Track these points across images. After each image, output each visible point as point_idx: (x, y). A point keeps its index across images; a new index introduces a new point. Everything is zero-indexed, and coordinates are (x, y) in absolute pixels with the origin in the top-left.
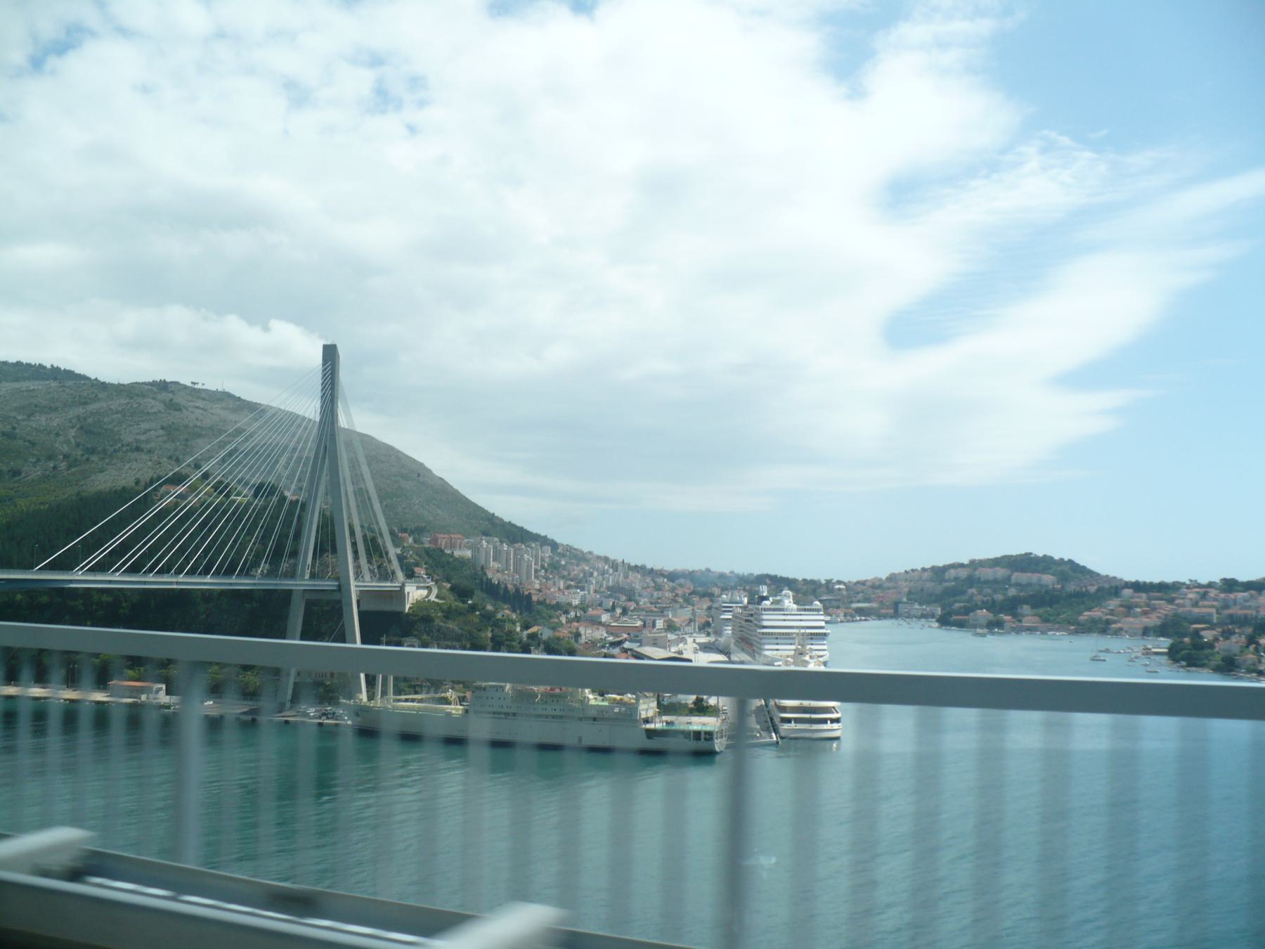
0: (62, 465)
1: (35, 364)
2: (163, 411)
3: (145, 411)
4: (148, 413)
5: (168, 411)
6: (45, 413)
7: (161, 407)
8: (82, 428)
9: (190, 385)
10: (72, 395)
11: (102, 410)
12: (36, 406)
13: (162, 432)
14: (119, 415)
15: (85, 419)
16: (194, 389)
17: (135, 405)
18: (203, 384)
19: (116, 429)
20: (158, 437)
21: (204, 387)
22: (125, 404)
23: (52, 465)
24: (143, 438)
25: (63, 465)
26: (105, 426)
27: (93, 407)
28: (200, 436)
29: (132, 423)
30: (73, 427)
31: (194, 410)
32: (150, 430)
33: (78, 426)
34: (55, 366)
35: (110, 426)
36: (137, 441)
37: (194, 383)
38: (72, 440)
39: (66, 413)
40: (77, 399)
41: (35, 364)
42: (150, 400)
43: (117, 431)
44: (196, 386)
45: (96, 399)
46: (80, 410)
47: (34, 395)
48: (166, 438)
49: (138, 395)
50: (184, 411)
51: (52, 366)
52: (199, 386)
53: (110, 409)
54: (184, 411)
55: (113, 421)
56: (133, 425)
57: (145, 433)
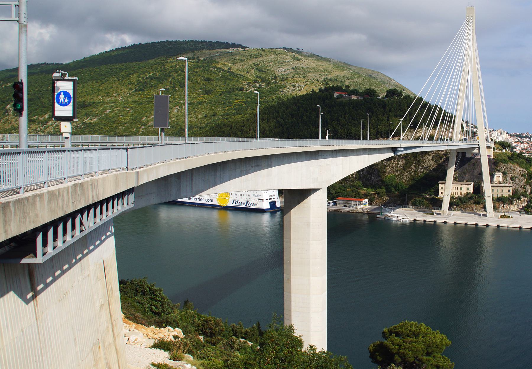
0: (263, 85)
1: (225, 42)
2: (292, 61)
3: (284, 61)
4: (285, 62)
5: (294, 61)
6: (239, 63)
7: (290, 59)
8: (257, 69)
9: (297, 50)
10: (249, 54)
11: (264, 61)
12: (235, 59)
13: (293, 71)
14: (273, 63)
15: (258, 65)
16: (299, 52)
17: (279, 59)
18: (302, 49)
19: (272, 70)
20: (292, 73)
21: (303, 51)
22: (274, 58)
23: (258, 85)
24: (285, 73)
25: (264, 85)
26: (267, 68)
27: (260, 59)
28: (310, 72)
29: (279, 67)
30: (253, 69)
31: (305, 60)
32: (287, 70)
33: (255, 68)
34: (233, 43)
35: (269, 68)
36: (283, 75)
37: (297, 49)
38: (254, 75)
39: (248, 62)
40: (252, 56)
41: (225, 42)
42: (286, 56)
43: (273, 70)
44: (299, 50)
45: (261, 56)
46: (255, 61)
47: (232, 54)
48: (295, 73)
49: (279, 53)
50: (301, 61)
51: (232, 43)
52: (301, 50)
53: (269, 60)
54: (301, 61)
55: (270, 66)
56: (280, 68)
57: (285, 71)
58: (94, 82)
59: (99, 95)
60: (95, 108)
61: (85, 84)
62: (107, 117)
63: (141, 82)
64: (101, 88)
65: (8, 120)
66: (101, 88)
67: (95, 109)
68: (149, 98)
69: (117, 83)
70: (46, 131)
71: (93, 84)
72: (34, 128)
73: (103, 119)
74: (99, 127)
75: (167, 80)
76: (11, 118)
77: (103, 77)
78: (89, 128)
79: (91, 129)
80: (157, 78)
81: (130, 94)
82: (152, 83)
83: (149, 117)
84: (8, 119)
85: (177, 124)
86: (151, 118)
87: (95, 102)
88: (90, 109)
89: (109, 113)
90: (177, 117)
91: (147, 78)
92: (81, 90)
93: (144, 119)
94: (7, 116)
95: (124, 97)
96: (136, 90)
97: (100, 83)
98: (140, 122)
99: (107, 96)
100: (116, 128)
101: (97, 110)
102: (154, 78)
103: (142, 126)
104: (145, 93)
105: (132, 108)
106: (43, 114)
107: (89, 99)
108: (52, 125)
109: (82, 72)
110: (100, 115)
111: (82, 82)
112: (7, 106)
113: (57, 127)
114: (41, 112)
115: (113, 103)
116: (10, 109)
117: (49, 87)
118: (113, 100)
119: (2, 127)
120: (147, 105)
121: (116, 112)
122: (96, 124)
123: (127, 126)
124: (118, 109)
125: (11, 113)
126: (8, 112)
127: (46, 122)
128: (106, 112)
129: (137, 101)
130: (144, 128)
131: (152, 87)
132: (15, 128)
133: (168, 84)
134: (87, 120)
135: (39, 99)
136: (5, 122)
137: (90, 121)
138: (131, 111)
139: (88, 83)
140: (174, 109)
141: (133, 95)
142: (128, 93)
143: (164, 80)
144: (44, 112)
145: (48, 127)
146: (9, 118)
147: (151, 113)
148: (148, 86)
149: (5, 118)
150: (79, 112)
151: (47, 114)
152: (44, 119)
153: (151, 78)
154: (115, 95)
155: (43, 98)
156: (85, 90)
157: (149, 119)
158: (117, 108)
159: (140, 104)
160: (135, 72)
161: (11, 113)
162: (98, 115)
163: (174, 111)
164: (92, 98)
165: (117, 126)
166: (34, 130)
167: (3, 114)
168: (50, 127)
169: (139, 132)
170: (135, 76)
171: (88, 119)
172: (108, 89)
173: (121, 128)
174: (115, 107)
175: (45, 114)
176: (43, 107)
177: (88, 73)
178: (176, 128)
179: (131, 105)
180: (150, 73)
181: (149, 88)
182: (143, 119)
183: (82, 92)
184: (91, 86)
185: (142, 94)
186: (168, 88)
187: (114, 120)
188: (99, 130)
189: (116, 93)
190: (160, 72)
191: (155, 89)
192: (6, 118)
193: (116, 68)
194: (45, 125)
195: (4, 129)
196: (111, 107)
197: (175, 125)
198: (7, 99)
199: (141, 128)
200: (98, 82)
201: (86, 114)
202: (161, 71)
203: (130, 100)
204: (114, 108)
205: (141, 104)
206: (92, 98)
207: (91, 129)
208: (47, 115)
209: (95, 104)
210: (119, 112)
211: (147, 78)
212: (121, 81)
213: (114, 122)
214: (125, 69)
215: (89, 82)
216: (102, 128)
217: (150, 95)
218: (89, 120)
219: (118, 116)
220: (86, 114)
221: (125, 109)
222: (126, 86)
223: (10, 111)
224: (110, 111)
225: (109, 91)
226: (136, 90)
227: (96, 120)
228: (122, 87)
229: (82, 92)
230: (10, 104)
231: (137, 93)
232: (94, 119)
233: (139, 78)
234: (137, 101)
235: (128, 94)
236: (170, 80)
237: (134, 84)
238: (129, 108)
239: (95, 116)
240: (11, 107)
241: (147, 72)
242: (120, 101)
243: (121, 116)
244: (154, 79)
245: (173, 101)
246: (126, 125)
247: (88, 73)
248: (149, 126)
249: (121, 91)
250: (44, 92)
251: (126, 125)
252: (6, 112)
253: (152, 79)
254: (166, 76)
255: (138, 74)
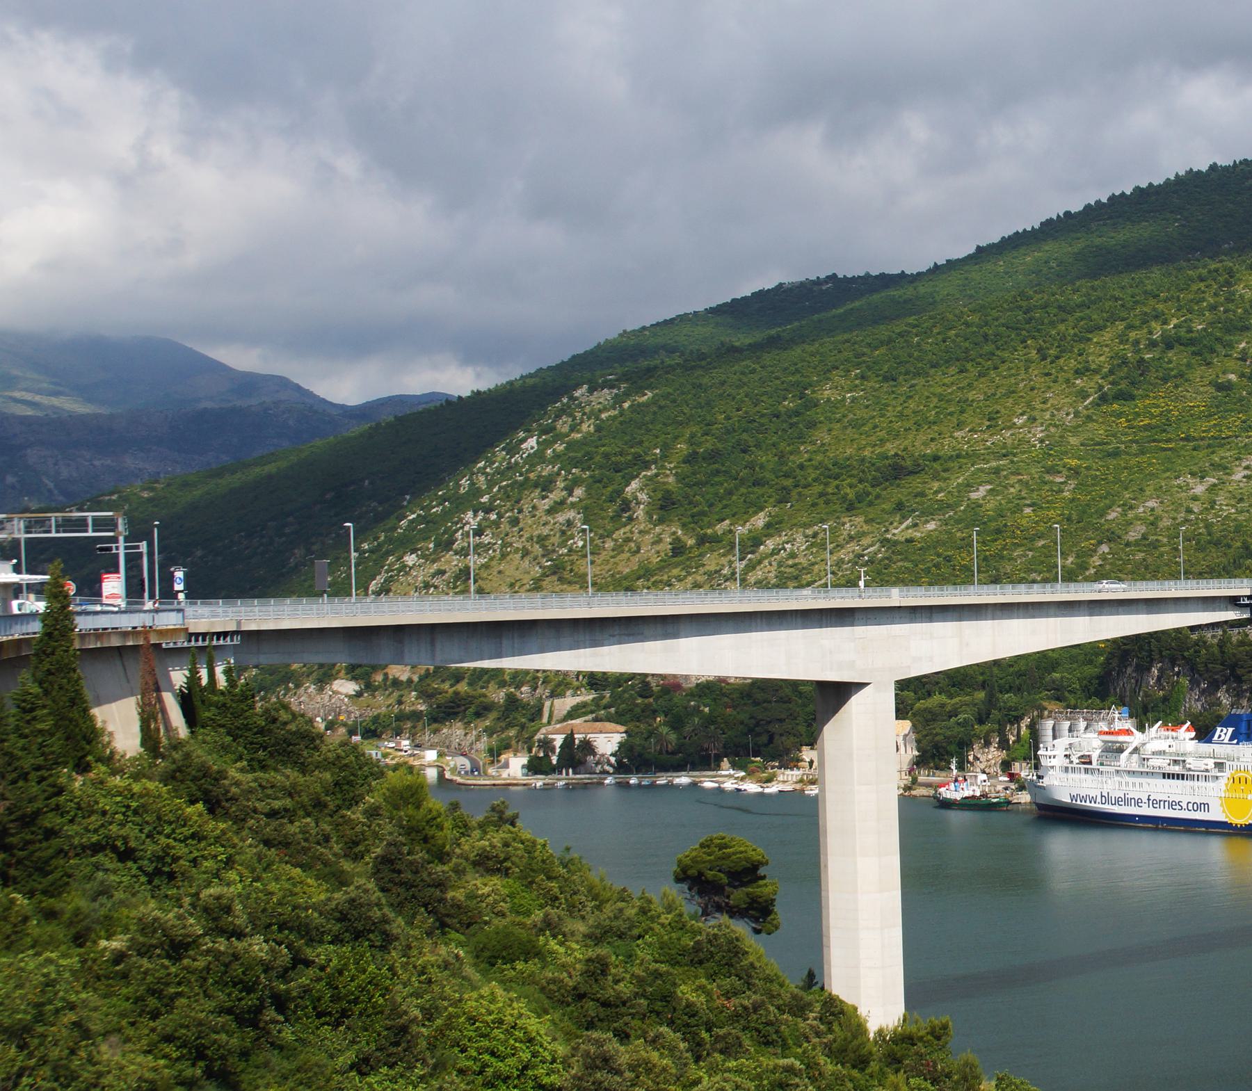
58: (953, 370)
59: (959, 426)
60: (936, 477)
61: (919, 381)
62: (974, 515)
63: (1125, 362)
64: (971, 395)
65: (628, 540)
66: (971, 395)
67: (936, 485)
68: (1148, 428)
69: (1034, 371)
70: (752, 578)
71: (945, 381)
72: (713, 568)
73: (958, 522)
74: (939, 555)
75: (1230, 345)
76: (640, 532)
77: (989, 348)
78: (902, 560)
79: (907, 564)
80: (1192, 342)
81: (1077, 414)
82: (1170, 362)
83: (1131, 508)
84: (629, 535)
85: (1238, 530)
86: (1141, 510)
87: (941, 454)
88: (916, 483)
89: (984, 498)
90: (1241, 500)
91: (1153, 344)
92: (900, 408)
93: (1112, 515)
94: (625, 526)
95: (1053, 430)
96: (1104, 399)
97: (973, 371)
98: (1097, 529)
99: (988, 427)
100: (1002, 557)
101: (943, 485)
102: (1179, 341)
103: (1100, 543)
104: (1136, 406)
105: (1075, 472)
106: (751, 510)
107: (919, 444)
108: (775, 552)
109: (914, 331)
110: (949, 506)
111: (907, 373)
112: (628, 484)
113: (790, 562)
114: (745, 501)
115: (1004, 456)
116: (636, 498)
117: (785, 399)
118: (1009, 441)
119: (607, 568)
120: (1136, 455)
121: (1012, 490)
122: (932, 543)
123: (1043, 546)
124: (1021, 480)
125: (640, 513)
126: (629, 509)
127: (755, 541)
128: (974, 496)
129: (1099, 444)
130: (1107, 550)
131: (1165, 380)
132: (647, 570)
133: (1231, 364)
134: (900, 531)
135: (744, 451)
136: (618, 549)
137: (911, 533)
138: (1072, 484)
139: (927, 375)
140: (1236, 469)
141: (1089, 418)
142: (1071, 410)
143: (1219, 347)
144: (752, 504)
145: (760, 562)
146: (632, 532)
147: (1142, 490)
148: (1152, 376)
149: (620, 534)
150: (878, 497)
151: (762, 509)
152: (750, 531)
153: (1169, 343)
154: (1019, 421)
155: (758, 446)
156: (912, 404)
157: (1131, 514)
158: (1019, 474)
159: (1109, 455)
160: (1113, 319)
161: (640, 513)
162: (944, 507)
163: (1233, 477)
164: (932, 440)
165: (1004, 548)
166: (710, 575)
167: (612, 518)
168: (766, 562)
169: (1083, 567)
170: (1107, 335)
171: (903, 526)
172: (999, 395)
173: (1020, 556)
174: (1012, 473)
175: (756, 513)
176: (754, 485)
177: (935, 331)
178: (1229, 546)
179: (1074, 462)
180: (1165, 322)
181: (1155, 385)
182: (1109, 517)
183: (901, 416)
184: (939, 390)
185: (1120, 415)
186: (1229, 381)
187: (1001, 522)
188: (937, 566)
189: (1022, 414)
190: (1207, 314)
191: (1176, 387)
192: (622, 531)
193: (1045, 307)
194: (749, 556)
195: (612, 575)
196: (997, 471)
197: (1225, 537)
198: (629, 458)
199: (1095, 551)
200: (967, 371)
201: (900, 507)
202: (1213, 308)
203: (1073, 441)
204: (1006, 477)
205: (1115, 454)
206: (932, 440)
207: (907, 564)
208: (762, 514)
209: (936, 465)
210: (1023, 494)
211: (1153, 344)
212: (1052, 362)
213: (998, 531)
214: (1081, 306)
215: (932, 371)
216: (948, 559)
217: (1152, 416)
218: (907, 528)
219: (1018, 509)
220: (900, 507)
221: (1048, 477)
222: (1067, 381)
223: (638, 503)
224: (989, 487)
225: (998, 408)
226: (1104, 399)
227: (931, 526)
228: (1049, 387)
229: (901, 416)
230: (637, 476)
231: (1104, 408)
232: (927, 522)
233: (1122, 347)
234: (1099, 444)
235: (1068, 414)
236: (1243, 345)
237: (1096, 372)
238: (1065, 472)
239: (928, 513)
240: (642, 489)
241: (1156, 317)
242: (1035, 446)
243: (1029, 506)
244: (1177, 345)
245: (1237, 437)
246: (1041, 543)
247: (935, 331)
248: (1128, 544)
249: (1044, 403)
250: (763, 421)
251: (1041, 543)
252: (624, 510)
253: (1169, 346)
254: (1228, 331)
255: (1121, 326)
